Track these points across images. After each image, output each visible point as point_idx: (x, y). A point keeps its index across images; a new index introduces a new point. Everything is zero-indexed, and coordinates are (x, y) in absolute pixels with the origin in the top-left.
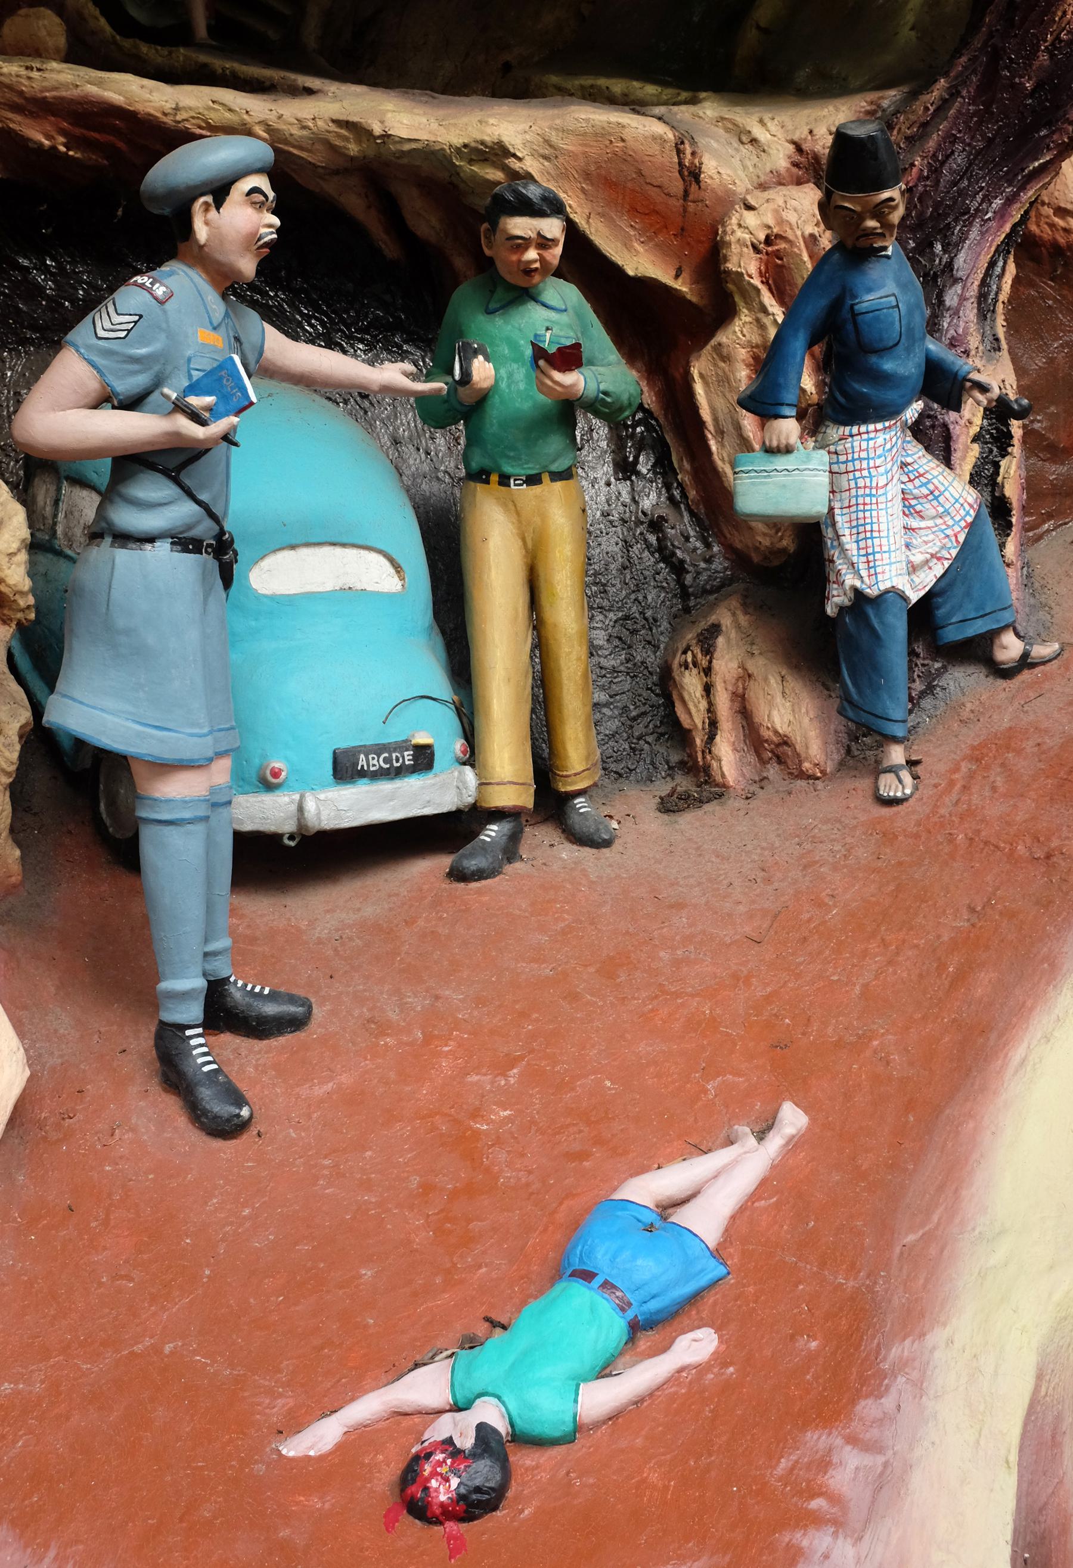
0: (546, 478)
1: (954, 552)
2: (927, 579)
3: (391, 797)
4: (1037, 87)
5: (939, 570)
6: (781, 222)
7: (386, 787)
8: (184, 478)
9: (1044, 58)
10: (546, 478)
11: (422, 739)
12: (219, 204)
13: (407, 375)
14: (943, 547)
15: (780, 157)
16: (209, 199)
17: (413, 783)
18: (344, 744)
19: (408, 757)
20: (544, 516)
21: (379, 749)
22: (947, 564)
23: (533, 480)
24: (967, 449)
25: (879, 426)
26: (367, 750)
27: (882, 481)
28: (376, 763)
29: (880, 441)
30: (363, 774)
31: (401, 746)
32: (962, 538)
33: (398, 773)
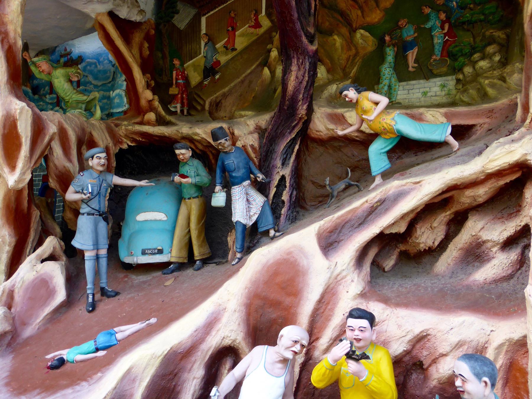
0: (192, 198)
1: (259, 212)
2: (254, 218)
3: (152, 258)
4: (288, 108)
5: (256, 216)
6: (245, 142)
7: (151, 257)
8: (88, 203)
9: (287, 103)
10: (192, 198)
11: (160, 248)
12: (92, 159)
13: (147, 182)
14: (257, 211)
15: (252, 128)
16: (91, 159)
17: (158, 256)
18: (144, 248)
19: (156, 251)
20: (191, 206)
21: (150, 249)
22: (258, 215)
23: (189, 199)
24: (273, 189)
25: (237, 186)
26: (148, 249)
27: (238, 198)
28: (149, 252)
29: (237, 190)
30: (146, 254)
31: (155, 249)
32: (260, 209)
33: (154, 254)
